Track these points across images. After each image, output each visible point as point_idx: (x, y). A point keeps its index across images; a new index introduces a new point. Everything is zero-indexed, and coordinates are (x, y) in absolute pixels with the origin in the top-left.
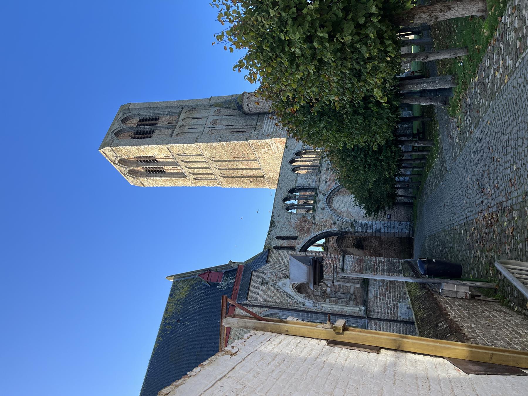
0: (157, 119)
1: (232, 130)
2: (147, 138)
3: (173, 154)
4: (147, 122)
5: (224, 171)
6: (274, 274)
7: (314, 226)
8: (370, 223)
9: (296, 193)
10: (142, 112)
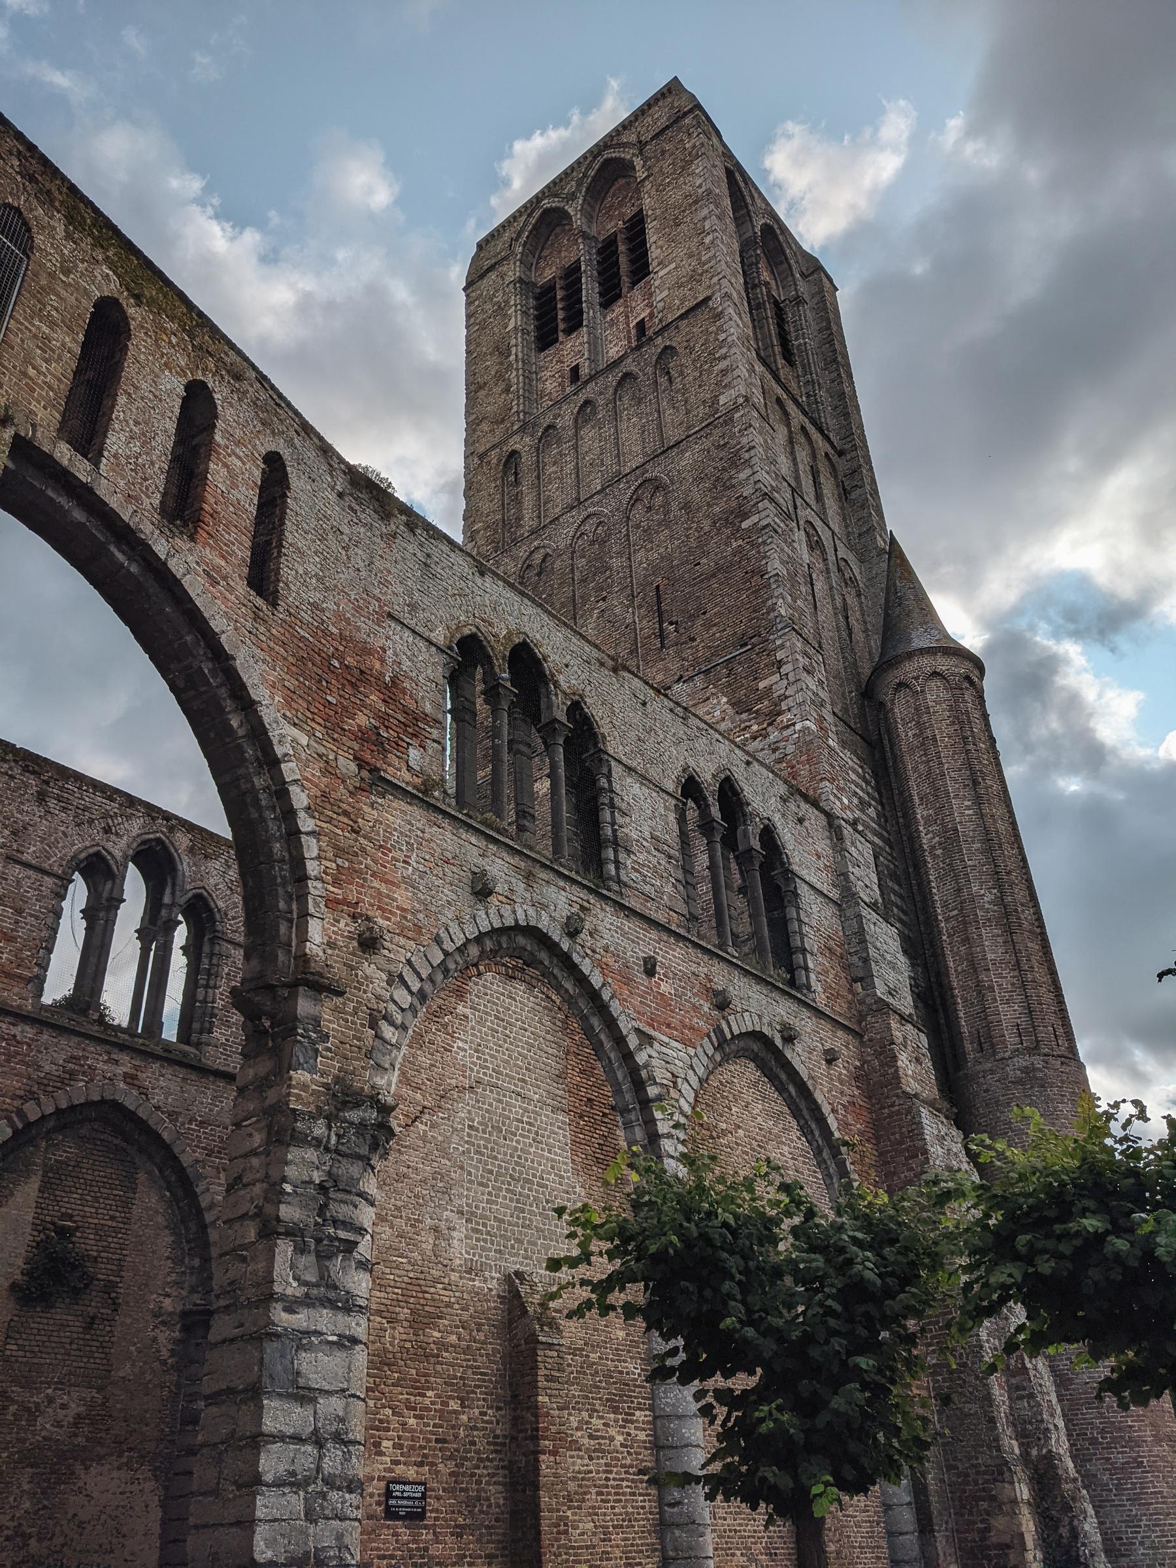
3: (672, 332)
7: (347, 765)
8: (360, 1284)
10: (808, 313)
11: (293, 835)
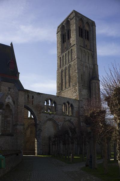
0: (88, 39)
1: (83, 75)
2: (79, 34)
4: (87, 35)
5: (64, 71)
6: (14, 93)
7: (39, 113)
9: (54, 105)
10: (91, 32)
11: (36, 118)
